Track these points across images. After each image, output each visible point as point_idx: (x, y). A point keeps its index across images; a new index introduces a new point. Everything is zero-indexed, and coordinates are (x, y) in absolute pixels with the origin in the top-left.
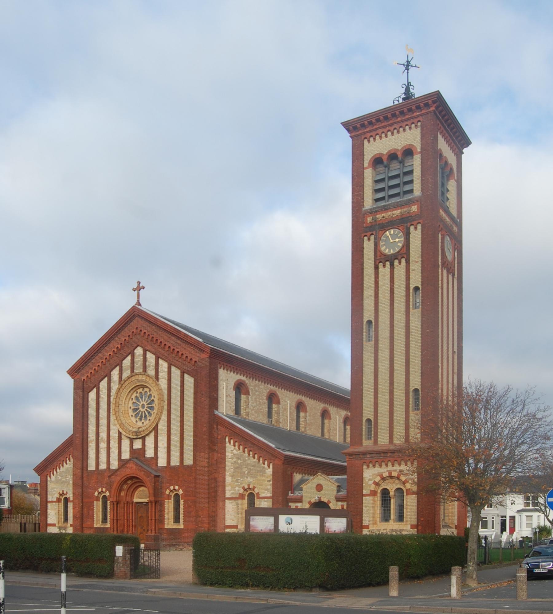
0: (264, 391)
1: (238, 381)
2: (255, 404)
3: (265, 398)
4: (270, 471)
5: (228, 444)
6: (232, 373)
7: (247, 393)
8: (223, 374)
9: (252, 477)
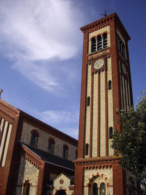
0: (47, 137)
1: (34, 130)
2: (42, 142)
3: (47, 140)
4: (38, 171)
5: (22, 157)
6: (31, 126)
7: (38, 136)
8: (25, 125)
9: (30, 174)
